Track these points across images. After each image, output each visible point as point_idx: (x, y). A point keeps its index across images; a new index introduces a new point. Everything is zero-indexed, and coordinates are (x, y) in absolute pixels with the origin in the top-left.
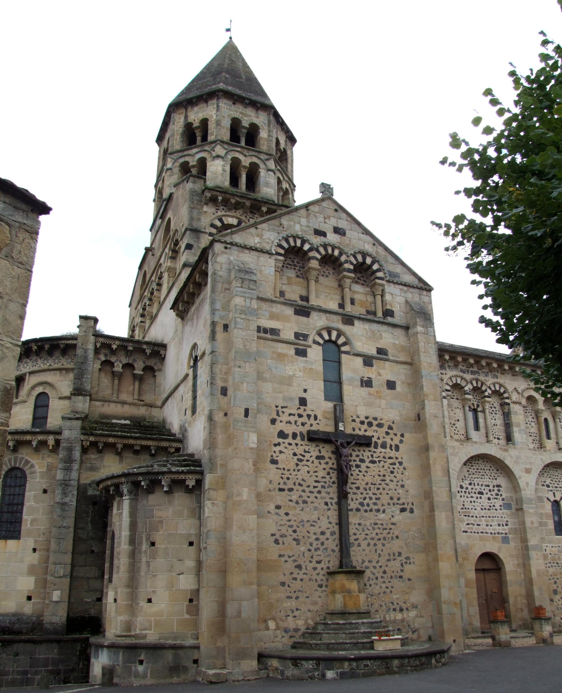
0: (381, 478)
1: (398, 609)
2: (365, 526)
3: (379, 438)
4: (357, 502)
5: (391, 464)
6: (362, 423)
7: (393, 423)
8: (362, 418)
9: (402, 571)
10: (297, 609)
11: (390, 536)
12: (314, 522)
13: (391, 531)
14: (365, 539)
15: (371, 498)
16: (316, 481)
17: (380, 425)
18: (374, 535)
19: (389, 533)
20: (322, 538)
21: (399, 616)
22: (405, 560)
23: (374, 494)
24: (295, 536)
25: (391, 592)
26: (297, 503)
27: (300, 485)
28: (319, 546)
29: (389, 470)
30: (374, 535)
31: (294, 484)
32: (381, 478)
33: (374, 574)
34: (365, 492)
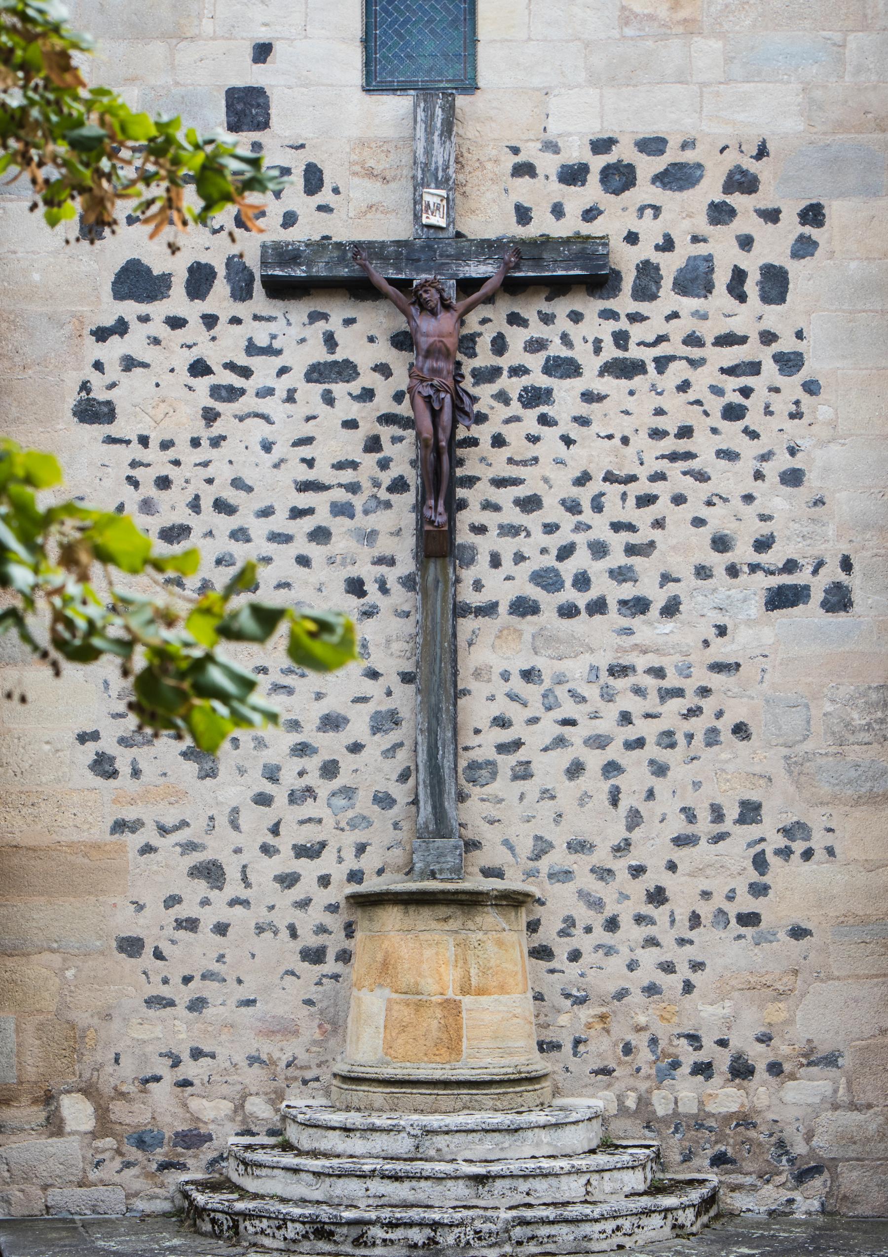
3: (668, 245)
7: (762, 152)
8: (576, 152)
10: (197, 1054)
11: (698, 725)
13: (709, 705)
14: (560, 742)
15: (599, 550)
17: (679, 177)
18: (607, 724)
25: (688, 987)
28: (313, 779)
29: (715, 405)
32: (669, 444)
33: (597, 904)
34: (567, 521)
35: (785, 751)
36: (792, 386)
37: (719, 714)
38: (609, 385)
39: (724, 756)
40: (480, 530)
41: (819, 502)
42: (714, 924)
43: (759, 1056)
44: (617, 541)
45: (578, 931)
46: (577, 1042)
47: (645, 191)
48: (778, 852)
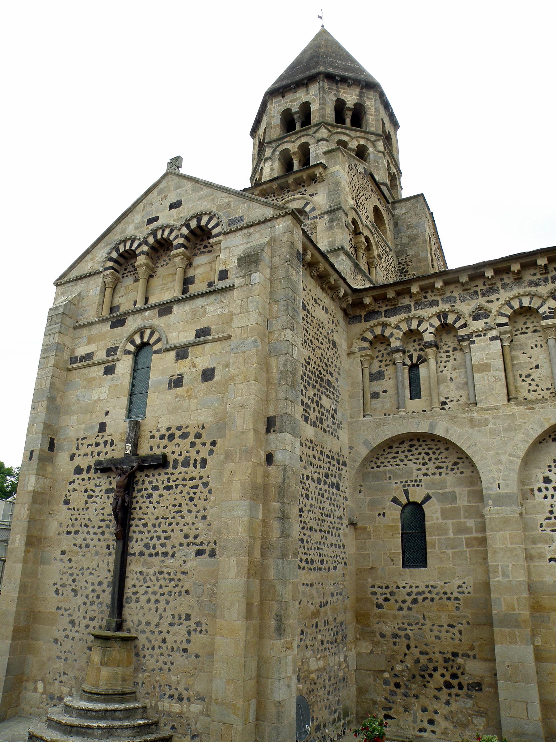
0: (176, 508)
1: (176, 696)
2: (148, 575)
3: (181, 454)
4: (143, 542)
5: (192, 488)
6: (162, 437)
7: (203, 427)
8: (163, 431)
9: (188, 641)
10: (64, 674)
11: (177, 590)
12: (93, 569)
13: (180, 584)
14: (146, 592)
15: (159, 538)
16: (103, 520)
17: (184, 436)
18: (156, 588)
19: (177, 586)
20: (99, 589)
21: (176, 707)
22: (194, 626)
23: (163, 532)
24: (73, 586)
25: (169, 670)
26: (80, 547)
27: (86, 526)
28: (95, 599)
29: (187, 497)
30: (156, 588)
31: (81, 525)
32: (176, 508)
33: (150, 641)
34: (153, 530)
35: (197, 599)
36: (205, 491)
37: (182, 587)
38: (165, 493)
39: (183, 599)
40: (134, 532)
41: (210, 525)
42: (177, 651)
43: (185, 694)
44: (163, 535)
45: (146, 649)
46: (143, 683)
47: (177, 440)
48: (194, 630)
